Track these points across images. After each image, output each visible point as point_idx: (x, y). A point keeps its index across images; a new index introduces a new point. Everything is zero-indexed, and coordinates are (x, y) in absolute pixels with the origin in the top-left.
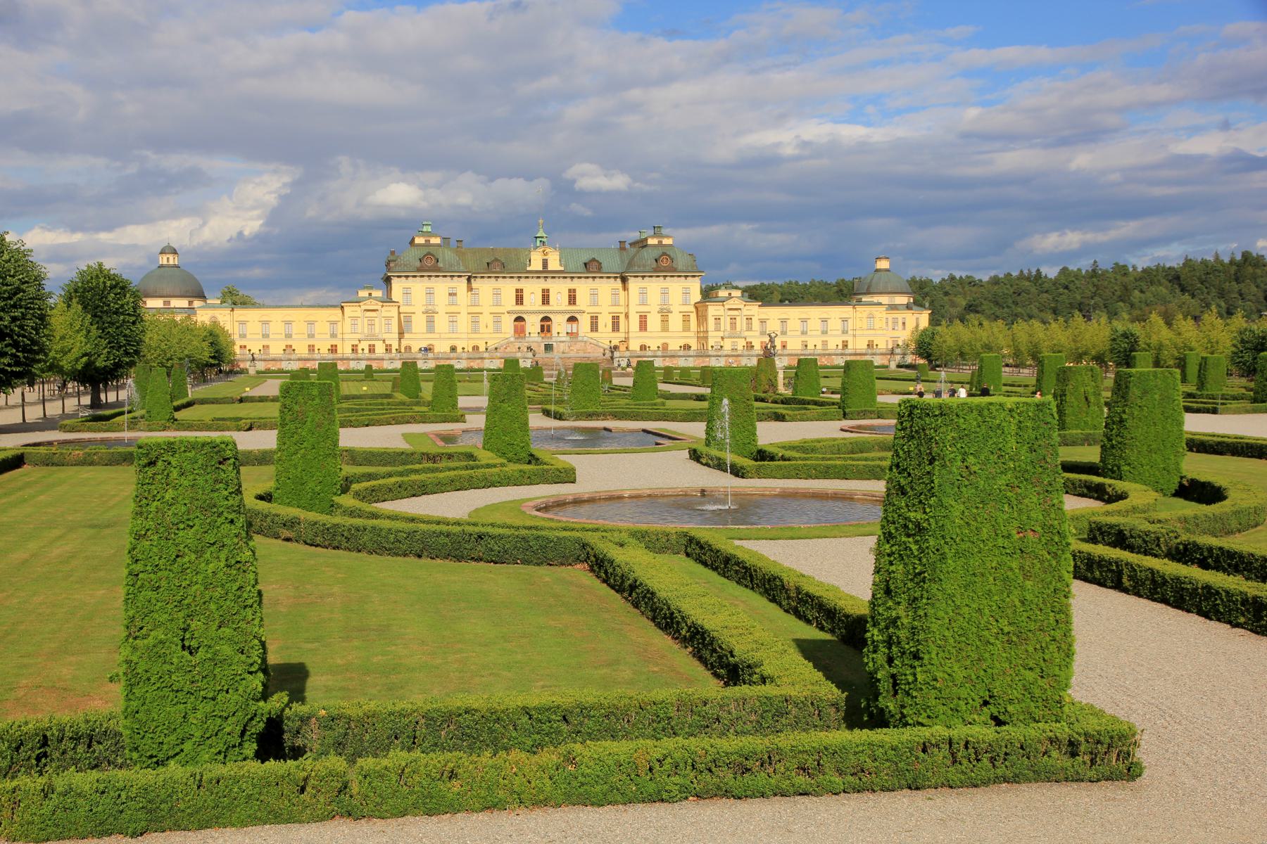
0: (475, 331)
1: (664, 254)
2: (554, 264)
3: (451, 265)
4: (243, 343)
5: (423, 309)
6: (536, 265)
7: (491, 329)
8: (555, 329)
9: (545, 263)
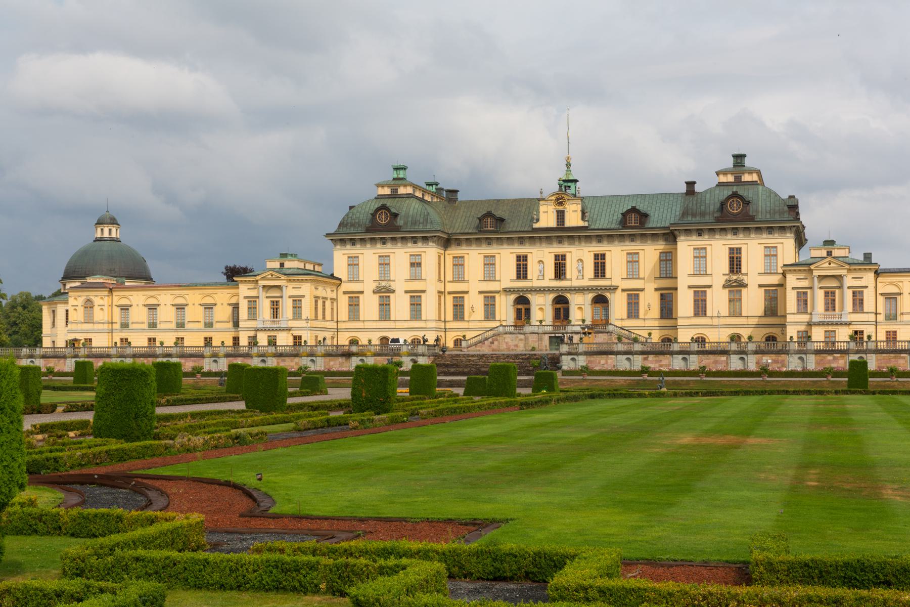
0: (459, 314)
1: (735, 195)
2: (573, 219)
3: (415, 223)
4: (124, 335)
5: (374, 286)
6: (547, 218)
7: (480, 314)
8: (575, 315)
9: (561, 215)
